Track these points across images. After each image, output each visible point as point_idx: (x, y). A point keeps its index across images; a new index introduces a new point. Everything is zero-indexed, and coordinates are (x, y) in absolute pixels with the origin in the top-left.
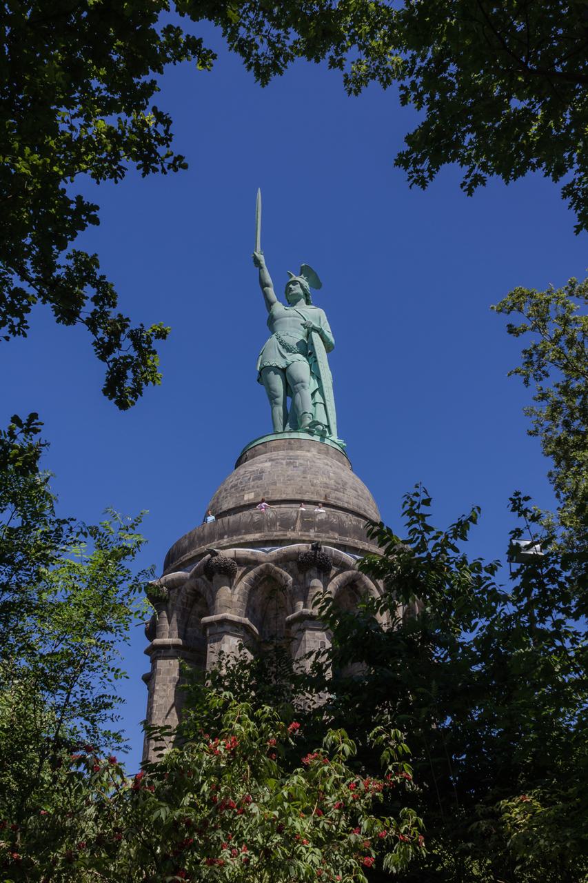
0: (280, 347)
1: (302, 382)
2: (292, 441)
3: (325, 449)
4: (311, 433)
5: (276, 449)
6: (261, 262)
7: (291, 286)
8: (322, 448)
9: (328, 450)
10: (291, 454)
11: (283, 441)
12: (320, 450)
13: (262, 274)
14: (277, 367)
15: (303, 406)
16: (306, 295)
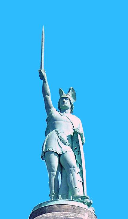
0: (59, 140)
1: (74, 167)
2: (76, 207)
3: (91, 215)
4: (84, 203)
5: (66, 210)
6: (45, 78)
7: (64, 100)
8: (90, 214)
9: (92, 215)
10: (77, 216)
11: (70, 206)
12: (89, 215)
13: (45, 86)
14: (57, 153)
15: (74, 182)
16: (72, 108)
